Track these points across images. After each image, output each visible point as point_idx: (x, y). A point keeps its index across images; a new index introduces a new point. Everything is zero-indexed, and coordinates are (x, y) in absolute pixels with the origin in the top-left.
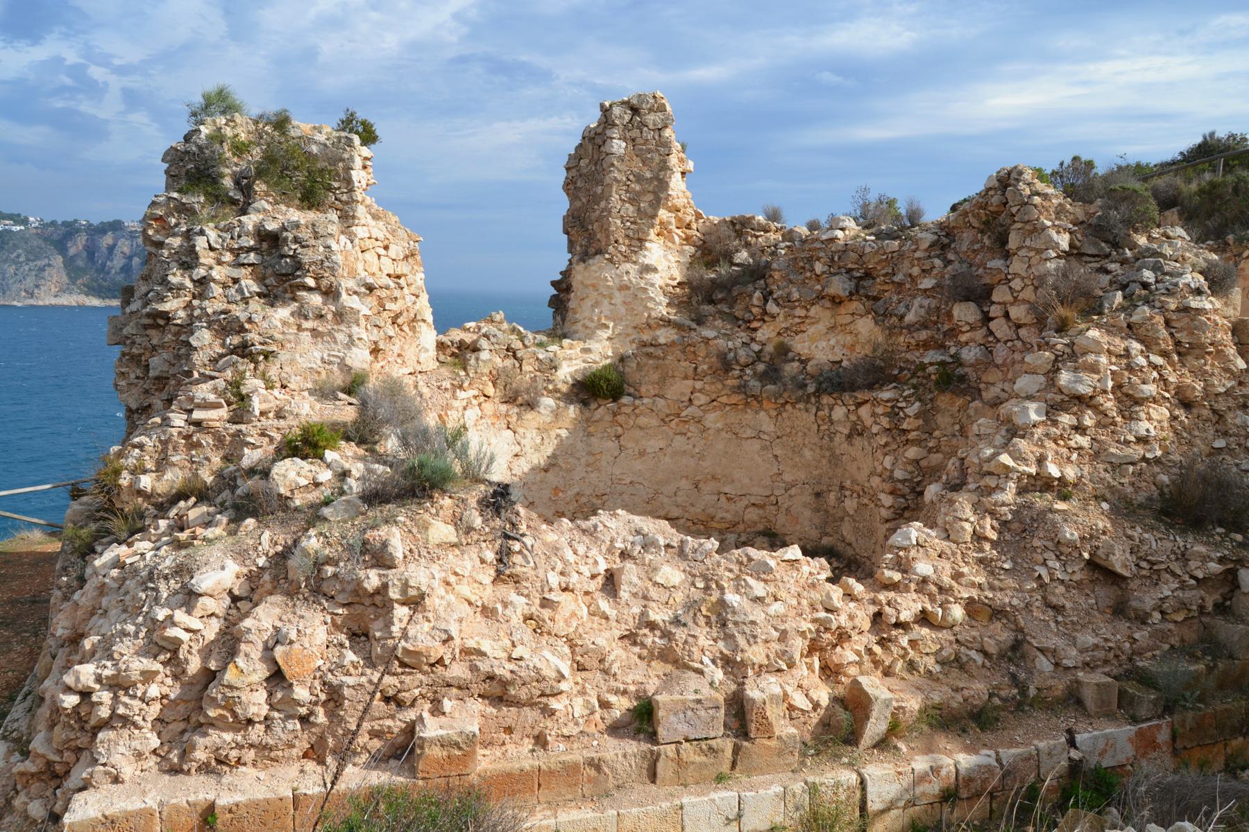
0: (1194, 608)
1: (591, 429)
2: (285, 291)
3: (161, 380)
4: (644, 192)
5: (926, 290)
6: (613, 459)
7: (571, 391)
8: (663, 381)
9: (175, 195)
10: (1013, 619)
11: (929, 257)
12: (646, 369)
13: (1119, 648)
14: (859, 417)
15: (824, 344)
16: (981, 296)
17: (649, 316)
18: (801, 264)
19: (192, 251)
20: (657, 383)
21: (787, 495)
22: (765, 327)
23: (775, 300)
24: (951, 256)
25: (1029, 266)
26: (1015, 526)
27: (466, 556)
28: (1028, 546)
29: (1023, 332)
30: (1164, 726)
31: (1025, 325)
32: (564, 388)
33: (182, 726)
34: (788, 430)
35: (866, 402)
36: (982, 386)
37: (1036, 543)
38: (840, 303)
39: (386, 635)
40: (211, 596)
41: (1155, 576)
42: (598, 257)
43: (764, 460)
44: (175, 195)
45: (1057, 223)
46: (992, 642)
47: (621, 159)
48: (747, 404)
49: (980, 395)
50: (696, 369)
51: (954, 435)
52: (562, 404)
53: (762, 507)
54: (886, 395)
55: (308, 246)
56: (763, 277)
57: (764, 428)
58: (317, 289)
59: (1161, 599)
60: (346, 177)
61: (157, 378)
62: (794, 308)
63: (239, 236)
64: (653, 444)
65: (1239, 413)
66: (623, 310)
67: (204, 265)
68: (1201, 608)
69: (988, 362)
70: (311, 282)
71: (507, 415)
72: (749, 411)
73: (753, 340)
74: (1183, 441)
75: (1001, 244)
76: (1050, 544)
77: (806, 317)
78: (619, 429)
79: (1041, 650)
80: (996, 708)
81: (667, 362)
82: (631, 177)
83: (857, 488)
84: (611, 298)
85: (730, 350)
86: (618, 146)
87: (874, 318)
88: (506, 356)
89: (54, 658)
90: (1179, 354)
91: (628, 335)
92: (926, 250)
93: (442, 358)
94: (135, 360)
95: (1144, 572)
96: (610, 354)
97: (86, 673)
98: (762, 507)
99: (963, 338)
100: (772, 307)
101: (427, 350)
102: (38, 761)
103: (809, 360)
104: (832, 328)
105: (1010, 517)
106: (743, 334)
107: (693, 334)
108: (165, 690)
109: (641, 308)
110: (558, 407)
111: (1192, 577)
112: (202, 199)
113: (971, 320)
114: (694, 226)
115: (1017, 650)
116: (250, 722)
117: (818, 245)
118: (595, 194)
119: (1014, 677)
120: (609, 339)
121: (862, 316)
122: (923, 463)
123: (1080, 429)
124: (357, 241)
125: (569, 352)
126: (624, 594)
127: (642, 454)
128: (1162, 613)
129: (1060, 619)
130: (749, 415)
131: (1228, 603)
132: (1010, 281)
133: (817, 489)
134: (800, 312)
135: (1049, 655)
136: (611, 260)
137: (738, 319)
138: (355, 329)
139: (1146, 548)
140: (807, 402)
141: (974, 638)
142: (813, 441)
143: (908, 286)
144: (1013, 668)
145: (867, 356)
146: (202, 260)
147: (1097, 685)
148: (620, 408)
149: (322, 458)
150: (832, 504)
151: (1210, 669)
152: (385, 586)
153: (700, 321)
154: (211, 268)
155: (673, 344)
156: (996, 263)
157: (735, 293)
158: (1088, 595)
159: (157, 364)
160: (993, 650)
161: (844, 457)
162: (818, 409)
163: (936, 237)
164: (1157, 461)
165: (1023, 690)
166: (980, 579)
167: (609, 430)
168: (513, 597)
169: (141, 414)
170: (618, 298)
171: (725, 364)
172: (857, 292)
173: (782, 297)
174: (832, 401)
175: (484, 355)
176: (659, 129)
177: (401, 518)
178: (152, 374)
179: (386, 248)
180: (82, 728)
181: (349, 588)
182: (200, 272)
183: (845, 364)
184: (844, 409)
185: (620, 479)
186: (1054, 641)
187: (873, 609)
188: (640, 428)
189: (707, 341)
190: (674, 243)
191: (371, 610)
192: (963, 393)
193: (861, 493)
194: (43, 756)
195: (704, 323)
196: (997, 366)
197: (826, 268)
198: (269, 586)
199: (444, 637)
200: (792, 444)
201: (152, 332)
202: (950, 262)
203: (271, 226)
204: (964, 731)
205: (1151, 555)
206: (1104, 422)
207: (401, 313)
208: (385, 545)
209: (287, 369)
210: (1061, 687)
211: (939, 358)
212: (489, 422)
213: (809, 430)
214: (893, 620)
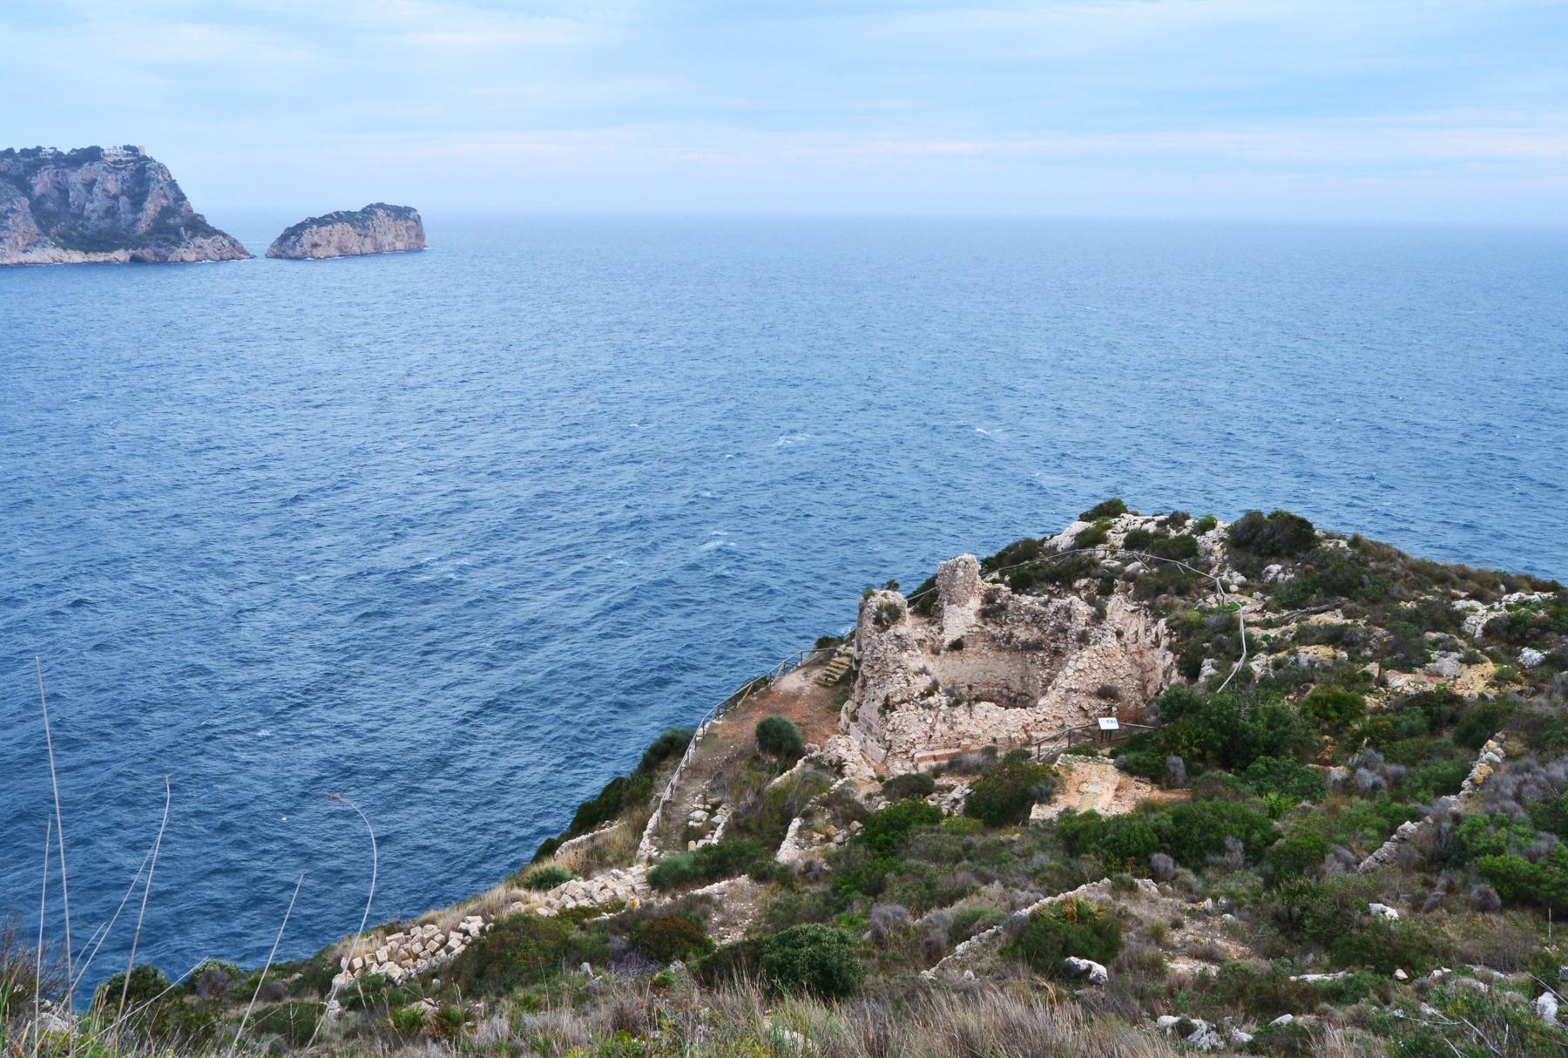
69: (1066, 648)
86: (960, 573)
115: (1063, 726)
159: (876, 667)
171: (994, 638)
206: (1086, 674)
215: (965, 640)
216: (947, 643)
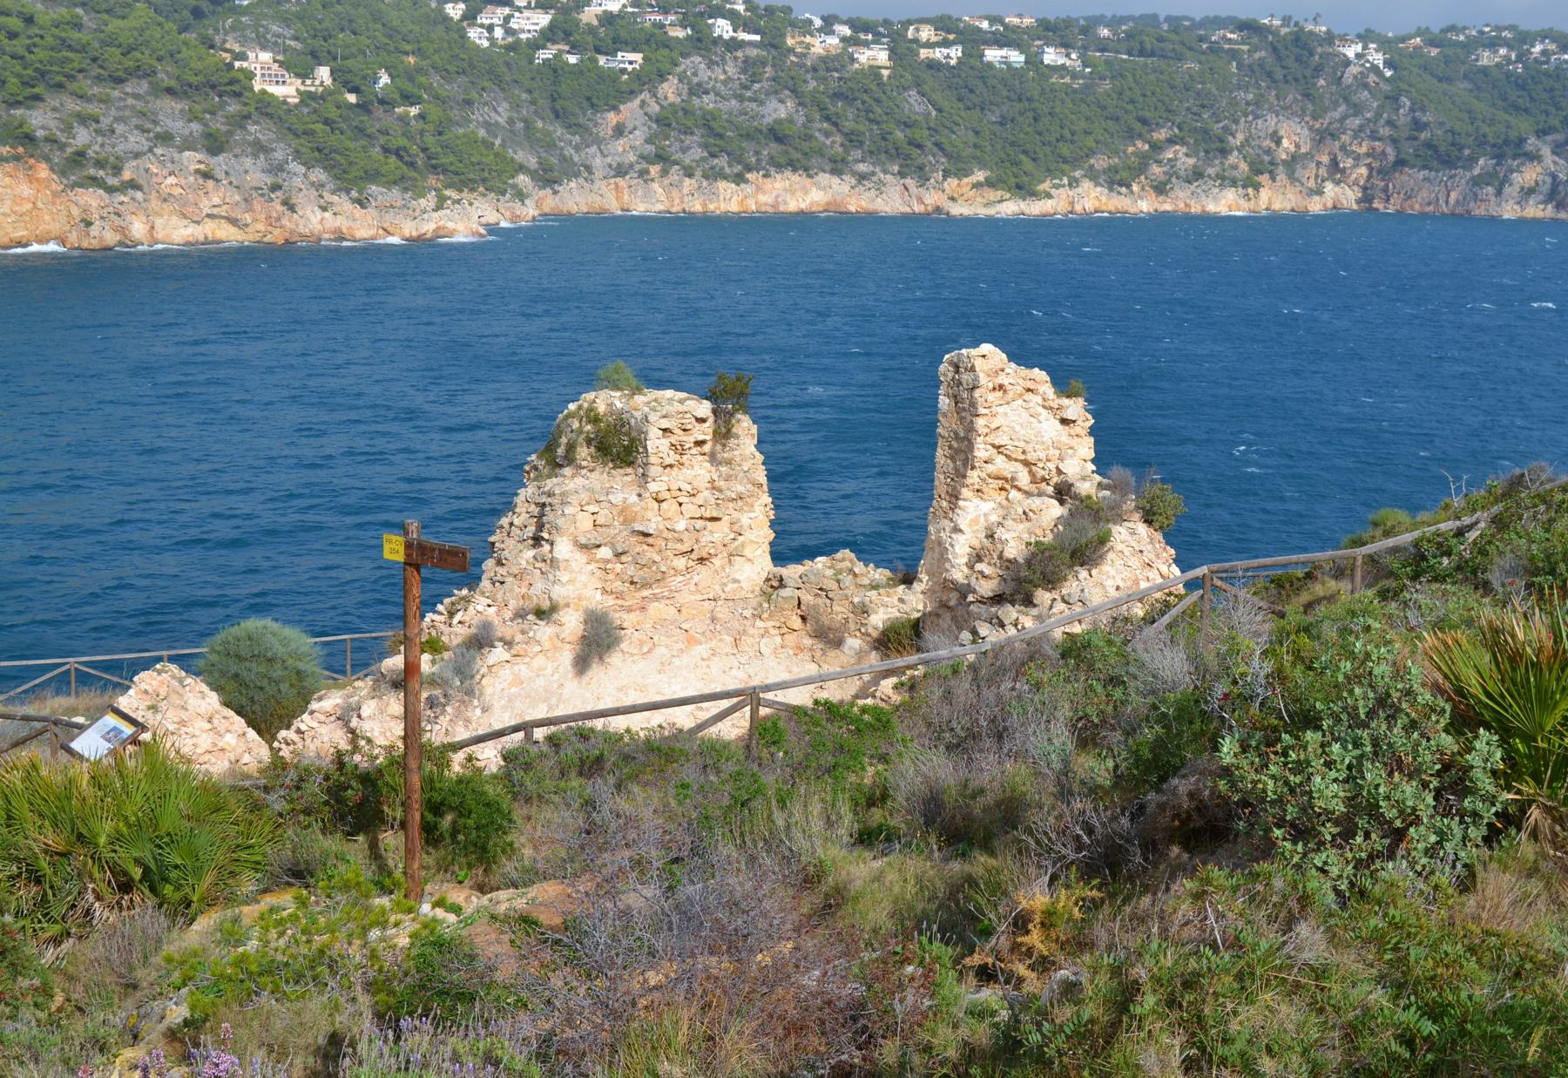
32: (875, 634)
47: (945, 415)
52: (867, 648)
70: (545, 535)
71: (811, 650)
91: (934, 592)
96: (921, 607)
101: (736, 581)
120: (922, 592)
125: (886, 599)
138: (558, 573)
170: (937, 549)
212: (791, 652)
216: (878, 620)
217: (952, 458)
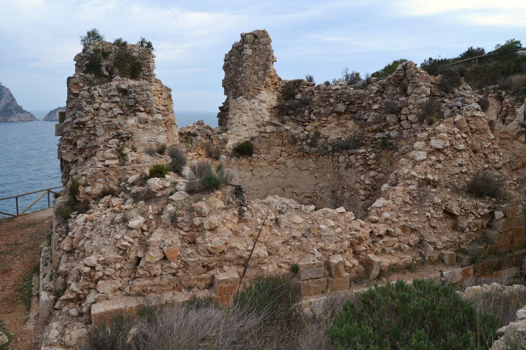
0: (480, 226)
1: (241, 168)
2: (131, 113)
3: (82, 150)
4: (260, 70)
5: (375, 110)
6: (249, 180)
7: (232, 152)
8: (269, 148)
9: (82, 74)
10: (419, 232)
11: (376, 96)
12: (262, 142)
13: (455, 241)
14: (350, 160)
15: (334, 131)
16: (396, 111)
17: (263, 121)
18: (324, 99)
19: (92, 97)
20: (267, 149)
21: (321, 192)
22: (310, 125)
23: (314, 114)
24: (385, 96)
25: (416, 100)
26: (418, 198)
27: (228, 213)
28: (423, 205)
29: (414, 126)
30: (472, 268)
31: (414, 123)
32: (230, 151)
33: (128, 279)
34: (321, 166)
35: (352, 154)
36: (398, 146)
37: (426, 204)
38: (340, 115)
39: (204, 242)
40: (136, 230)
41: (467, 215)
42: (241, 97)
43: (311, 179)
44: (82, 74)
45: (425, 84)
46: (412, 241)
48: (304, 156)
49: (398, 150)
50: (282, 142)
51: (388, 166)
53: (310, 197)
54: (362, 151)
55: (140, 94)
56: (308, 104)
57: (311, 165)
58: (145, 111)
59: (469, 223)
60: (148, 65)
61: (80, 149)
62: (322, 117)
63: (111, 91)
64: (266, 173)
65: (492, 155)
66: (252, 118)
67: (98, 102)
68: (482, 226)
72: (304, 159)
73: (305, 130)
74: (474, 165)
75: (404, 92)
76: (431, 204)
77: (327, 120)
78: (252, 167)
79: (429, 243)
80: (415, 264)
81: (271, 139)
82: (254, 64)
83: (349, 188)
84: (247, 114)
85: (296, 134)
86: (249, 52)
87: (354, 120)
88: (206, 138)
89: (60, 259)
90: (472, 133)
92: (374, 94)
93: (181, 139)
94: (70, 142)
95: (463, 214)
97: (93, 259)
98: (310, 197)
99: (391, 128)
100: (313, 117)
102: (74, 294)
103: (328, 138)
104: (337, 125)
105: (416, 195)
106: (301, 128)
107: (281, 128)
108: (122, 265)
109: (259, 118)
110: (227, 158)
111: (479, 215)
112: (93, 76)
113: (394, 121)
114: (278, 84)
115: (421, 243)
116: (155, 276)
117: (331, 91)
118: (239, 71)
119: (420, 253)
121: (349, 120)
122: (376, 177)
123: (439, 161)
124: (152, 91)
126: (282, 226)
127: (261, 177)
128: (469, 228)
129: (435, 231)
130: (304, 161)
131: (491, 224)
132: (408, 106)
133: (333, 189)
134: (324, 118)
135: (432, 244)
136: (246, 98)
137: (299, 122)
139: (463, 204)
140: (329, 154)
141: (406, 240)
142: (331, 170)
143: (368, 107)
144: (420, 250)
145: (351, 136)
146: (97, 101)
147: (449, 254)
148: (252, 159)
149: (164, 177)
150: (339, 195)
151: (485, 248)
152: (202, 224)
153: (283, 122)
154: (101, 104)
155: (273, 132)
156: (403, 99)
157: (297, 111)
158: (444, 223)
159: (80, 143)
160: (412, 243)
161: (344, 176)
162: (333, 157)
163: (378, 89)
164: (466, 173)
165: (424, 259)
166: (407, 218)
167: (248, 168)
168: (246, 228)
169: (73, 164)
170: (250, 113)
171: (294, 140)
172: (347, 110)
173: (316, 112)
174: (338, 154)
175: (199, 138)
176: (266, 45)
177: (204, 199)
178: (78, 147)
179: (161, 94)
180: (91, 281)
181: (189, 225)
182: (96, 105)
183: (343, 139)
184: (344, 157)
185: (252, 188)
186: (434, 240)
187: (370, 230)
188: (260, 167)
189: (287, 130)
190: (271, 91)
191: (197, 233)
192: (391, 149)
193: (351, 190)
194: (75, 292)
195: (285, 123)
196: (404, 139)
197: (334, 101)
198: (155, 226)
199: (225, 242)
200: (323, 172)
201: (77, 130)
202: (384, 98)
203: (124, 87)
204: (405, 273)
205: (465, 207)
207: (168, 121)
208: (201, 208)
209: (136, 144)
210: (436, 256)
211: (382, 136)
213: (329, 166)
214: (377, 234)
215: (255, 143)
216: (231, 144)
217: (256, 73)
